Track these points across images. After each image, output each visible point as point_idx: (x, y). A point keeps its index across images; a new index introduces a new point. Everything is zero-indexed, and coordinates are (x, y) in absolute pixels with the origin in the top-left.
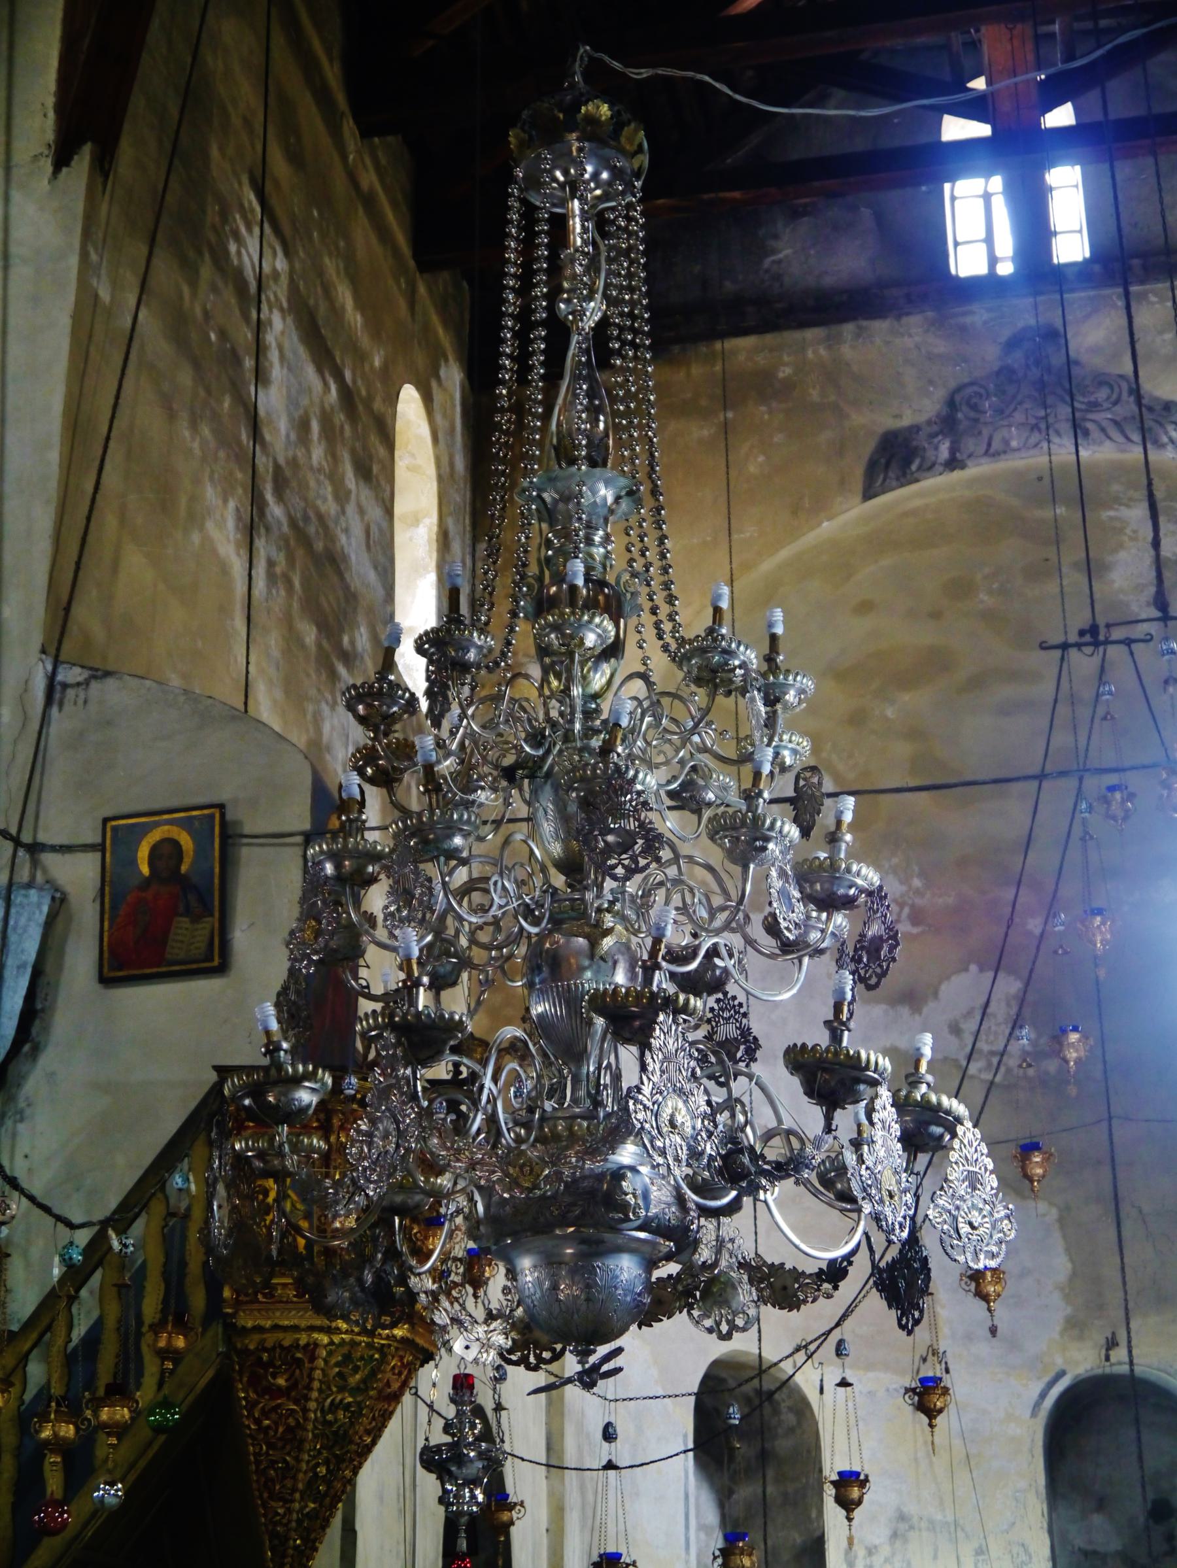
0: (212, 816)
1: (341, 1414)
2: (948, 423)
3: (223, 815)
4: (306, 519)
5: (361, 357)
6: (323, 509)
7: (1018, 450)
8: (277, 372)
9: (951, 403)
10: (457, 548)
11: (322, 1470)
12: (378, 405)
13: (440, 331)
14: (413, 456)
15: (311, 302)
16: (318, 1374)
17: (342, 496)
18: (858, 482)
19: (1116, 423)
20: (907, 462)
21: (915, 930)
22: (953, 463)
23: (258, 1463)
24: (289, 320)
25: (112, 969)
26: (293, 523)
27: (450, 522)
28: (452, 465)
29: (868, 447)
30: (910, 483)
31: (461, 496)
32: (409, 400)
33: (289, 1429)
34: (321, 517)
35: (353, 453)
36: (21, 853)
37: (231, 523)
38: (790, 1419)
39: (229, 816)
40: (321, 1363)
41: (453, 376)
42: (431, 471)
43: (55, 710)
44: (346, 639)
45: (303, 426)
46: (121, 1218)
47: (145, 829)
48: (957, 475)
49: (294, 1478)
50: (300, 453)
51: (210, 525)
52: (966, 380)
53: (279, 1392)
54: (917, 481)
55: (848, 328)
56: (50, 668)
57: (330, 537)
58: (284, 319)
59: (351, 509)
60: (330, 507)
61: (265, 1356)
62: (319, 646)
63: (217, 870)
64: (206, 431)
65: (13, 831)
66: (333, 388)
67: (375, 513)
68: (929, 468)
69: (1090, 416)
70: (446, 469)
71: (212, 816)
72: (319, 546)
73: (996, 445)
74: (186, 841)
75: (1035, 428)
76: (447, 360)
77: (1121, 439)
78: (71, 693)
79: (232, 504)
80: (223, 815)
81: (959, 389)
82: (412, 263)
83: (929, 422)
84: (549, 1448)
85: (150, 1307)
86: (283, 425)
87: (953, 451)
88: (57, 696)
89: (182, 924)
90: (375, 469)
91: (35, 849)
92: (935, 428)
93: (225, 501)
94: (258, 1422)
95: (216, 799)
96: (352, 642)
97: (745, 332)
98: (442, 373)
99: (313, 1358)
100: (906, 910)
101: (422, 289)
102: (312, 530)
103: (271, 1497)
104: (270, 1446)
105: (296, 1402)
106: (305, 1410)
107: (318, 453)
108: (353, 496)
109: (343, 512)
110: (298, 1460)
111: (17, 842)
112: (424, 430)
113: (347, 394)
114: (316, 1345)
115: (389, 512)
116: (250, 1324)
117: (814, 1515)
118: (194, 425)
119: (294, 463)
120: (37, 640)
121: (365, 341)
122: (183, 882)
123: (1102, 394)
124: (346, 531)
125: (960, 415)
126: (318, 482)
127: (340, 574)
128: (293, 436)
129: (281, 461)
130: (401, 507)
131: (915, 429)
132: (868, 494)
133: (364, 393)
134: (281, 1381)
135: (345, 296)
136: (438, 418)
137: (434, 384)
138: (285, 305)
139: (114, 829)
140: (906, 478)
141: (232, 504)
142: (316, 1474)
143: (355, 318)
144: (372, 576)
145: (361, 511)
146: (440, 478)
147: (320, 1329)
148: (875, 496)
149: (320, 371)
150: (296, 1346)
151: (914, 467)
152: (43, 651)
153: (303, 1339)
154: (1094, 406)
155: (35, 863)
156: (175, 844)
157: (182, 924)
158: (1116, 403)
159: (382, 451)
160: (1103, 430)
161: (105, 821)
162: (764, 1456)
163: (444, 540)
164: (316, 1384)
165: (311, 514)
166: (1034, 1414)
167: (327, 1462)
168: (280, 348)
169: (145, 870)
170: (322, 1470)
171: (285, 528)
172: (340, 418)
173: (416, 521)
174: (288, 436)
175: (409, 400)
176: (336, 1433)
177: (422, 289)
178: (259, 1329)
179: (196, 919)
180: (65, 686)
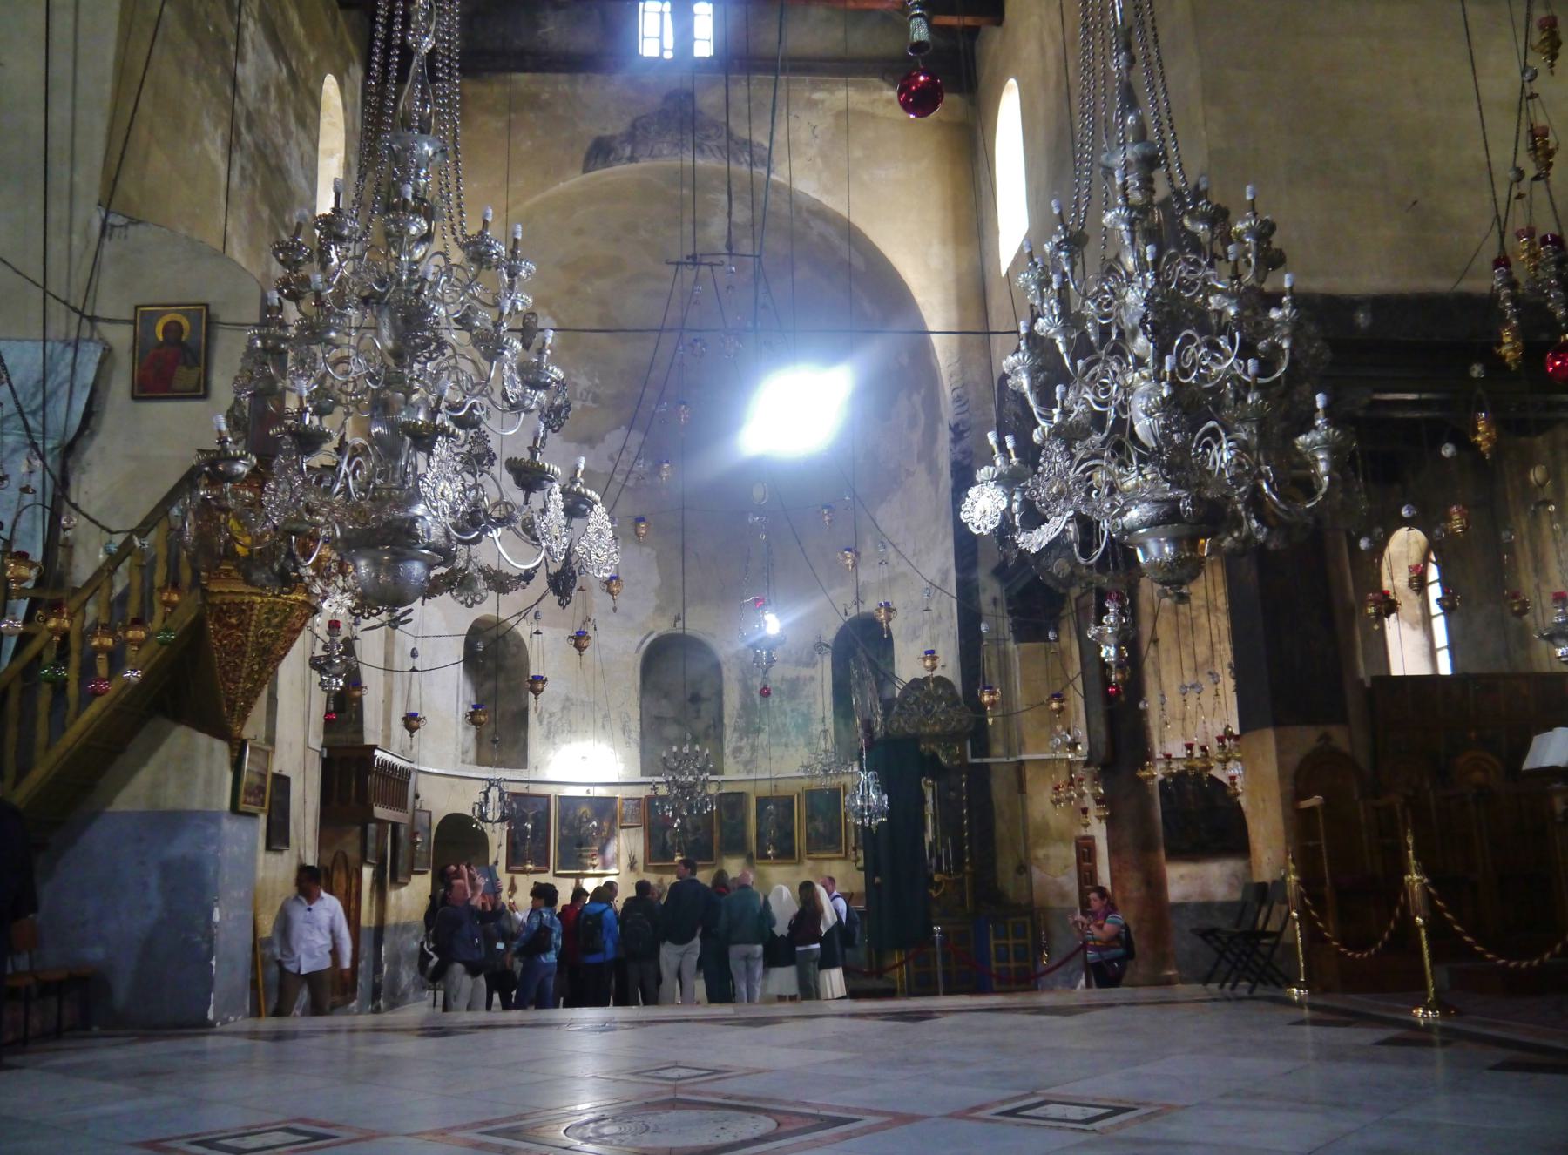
0: (201, 310)
1: (267, 639)
2: (631, 137)
3: (207, 310)
4: (265, 145)
5: (302, 54)
7: (667, 156)
8: (250, 56)
9: (634, 126)
11: (256, 667)
12: (311, 84)
14: (331, 116)
16: (254, 618)
17: (287, 134)
19: (718, 147)
21: (595, 406)
22: (632, 159)
23: (220, 663)
24: (259, 26)
26: (257, 146)
28: (354, 125)
29: (588, 143)
32: (330, 84)
33: (237, 646)
35: (295, 110)
36: (84, 321)
37: (219, 142)
38: (514, 650)
39: (212, 310)
40: (256, 612)
41: (357, 72)
42: (342, 126)
43: (106, 240)
44: (287, 218)
45: (265, 90)
46: (143, 530)
48: (633, 165)
49: (240, 671)
50: (263, 106)
51: (206, 142)
53: (232, 626)
54: (611, 166)
55: (581, 77)
56: (103, 214)
57: (278, 156)
58: (255, 24)
59: (292, 143)
60: (280, 140)
61: (225, 607)
62: (271, 221)
63: (203, 341)
64: (204, 84)
65: (80, 307)
66: (284, 70)
67: (307, 147)
68: (619, 160)
69: (707, 143)
70: (351, 127)
71: (201, 310)
72: (273, 162)
73: (656, 151)
74: (185, 323)
75: (676, 145)
76: (354, 63)
78: (117, 231)
83: (621, 135)
84: (386, 661)
85: (159, 578)
86: (253, 88)
88: (108, 231)
89: (182, 371)
90: (308, 121)
91: (93, 319)
93: (216, 128)
94: (220, 641)
95: (202, 301)
96: (291, 220)
97: (525, 70)
98: (351, 70)
99: (252, 610)
100: (590, 395)
102: (268, 151)
103: (227, 680)
104: (227, 654)
105: (242, 632)
106: (247, 636)
107: (274, 108)
108: (294, 135)
109: (288, 143)
110: (242, 662)
111: (82, 315)
112: (338, 102)
113: (293, 76)
114: (254, 602)
116: (216, 590)
117: (524, 697)
118: (197, 81)
119: (259, 111)
120: (96, 197)
121: (305, 44)
122: (183, 346)
123: (712, 132)
124: (290, 155)
125: (638, 133)
127: (285, 180)
128: (259, 95)
129: (251, 108)
130: (323, 145)
131: (613, 138)
132: (586, 170)
133: (303, 75)
134: (234, 621)
136: (348, 97)
137: (345, 76)
138: (256, 15)
139: (142, 312)
141: (220, 131)
142: (253, 670)
143: (299, 30)
144: (304, 183)
145: (299, 145)
146: (347, 131)
147: (257, 594)
149: (276, 57)
151: (611, 158)
152: (100, 204)
153: (247, 599)
154: (708, 137)
155: (93, 328)
156: (179, 325)
157: (182, 371)
159: (312, 111)
160: (711, 150)
161: (137, 307)
162: (499, 668)
164: (253, 623)
165: (268, 143)
166: (637, 651)
167: (259, 664)
168: (253, 42)
169: (160, 337)
170: (256, 667)
171: (252, 149)
172: (288, 88)
173: (331, 154)
174: (256, 94)
175: (330, 84)
176: (264, 649)
178: (221, 593)
180: (113, 226)
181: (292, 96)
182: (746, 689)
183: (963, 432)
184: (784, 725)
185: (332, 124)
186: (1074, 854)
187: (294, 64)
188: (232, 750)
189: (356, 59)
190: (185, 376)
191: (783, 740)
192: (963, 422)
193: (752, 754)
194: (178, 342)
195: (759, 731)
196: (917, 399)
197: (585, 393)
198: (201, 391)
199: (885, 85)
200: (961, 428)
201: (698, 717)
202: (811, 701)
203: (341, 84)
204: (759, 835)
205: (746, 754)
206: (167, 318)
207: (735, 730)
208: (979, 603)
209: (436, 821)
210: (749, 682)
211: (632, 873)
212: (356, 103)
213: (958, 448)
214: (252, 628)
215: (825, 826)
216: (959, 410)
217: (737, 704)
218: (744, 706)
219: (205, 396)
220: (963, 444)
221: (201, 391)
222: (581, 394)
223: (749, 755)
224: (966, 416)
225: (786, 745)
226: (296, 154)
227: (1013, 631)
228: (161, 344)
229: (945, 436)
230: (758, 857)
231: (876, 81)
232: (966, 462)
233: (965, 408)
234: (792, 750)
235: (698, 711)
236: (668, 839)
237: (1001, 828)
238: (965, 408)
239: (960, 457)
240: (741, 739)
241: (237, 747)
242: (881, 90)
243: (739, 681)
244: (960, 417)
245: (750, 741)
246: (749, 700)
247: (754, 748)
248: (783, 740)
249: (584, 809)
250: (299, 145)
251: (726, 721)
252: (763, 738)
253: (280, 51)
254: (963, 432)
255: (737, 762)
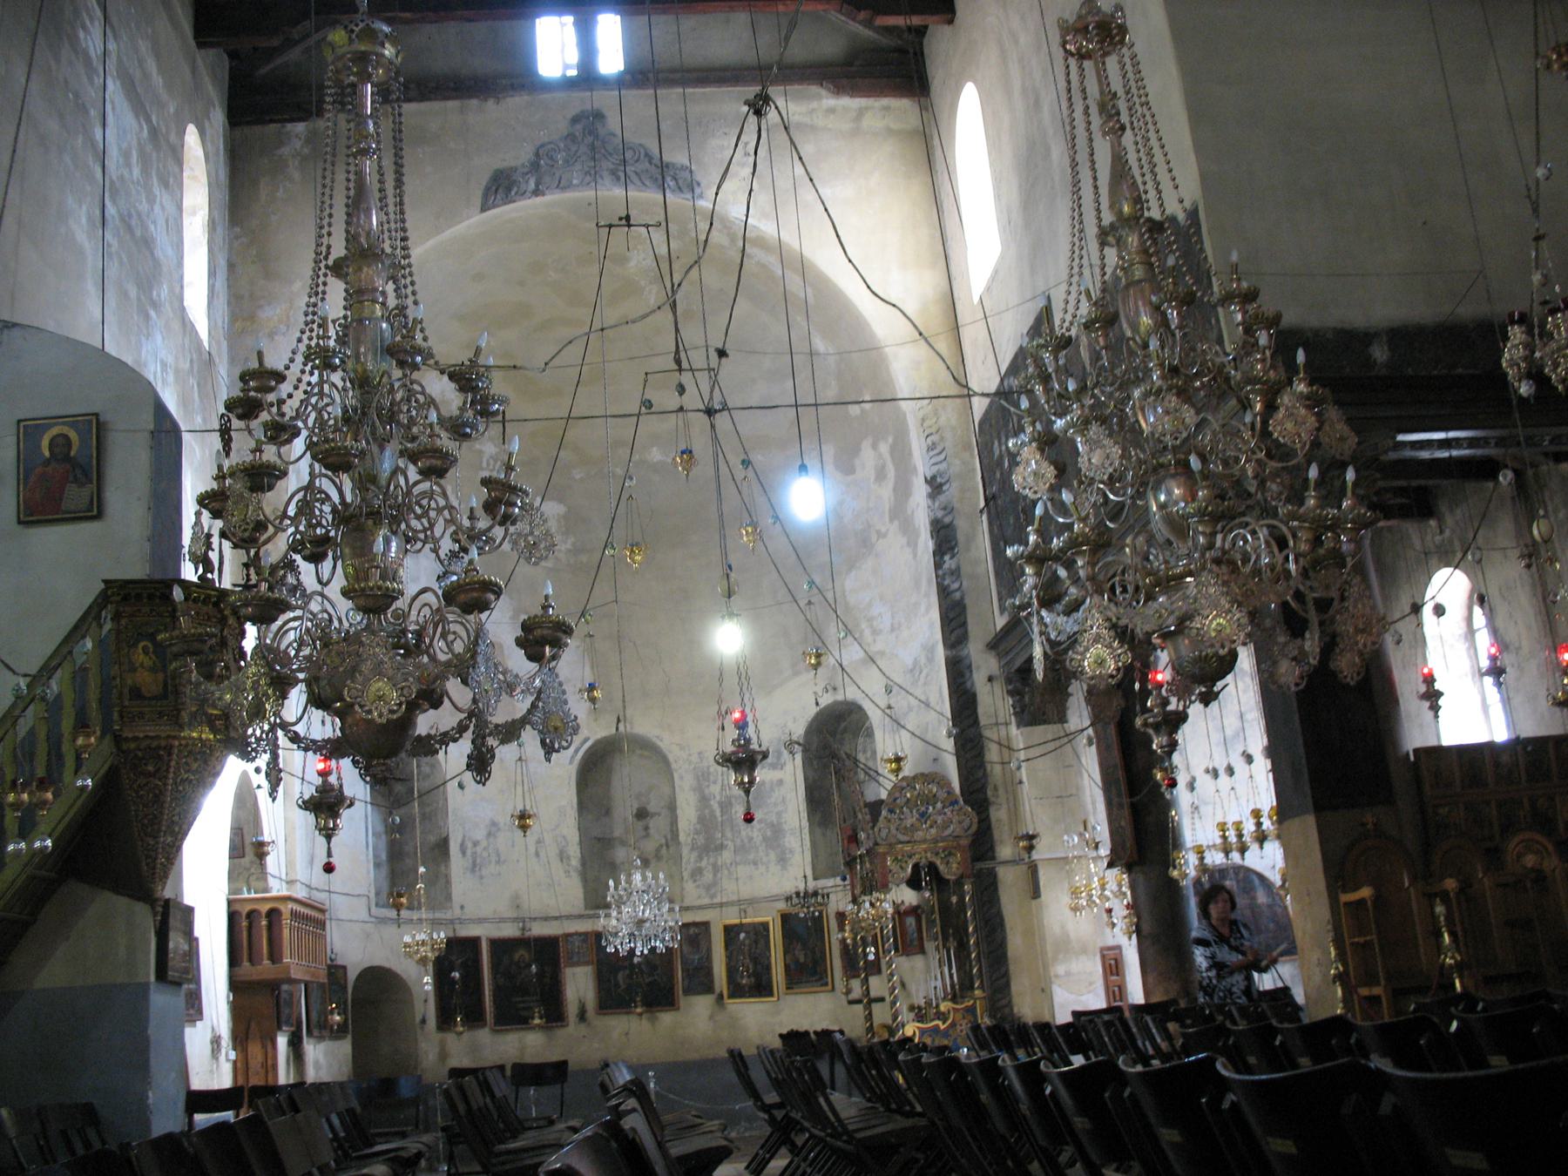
0: (90, 422)
2: (535, 166)
3: (98, 420)
4: (130, 216)
6: (140, 208)
9: (537, 155)
10: (219, 230)
12: (173, 138)
13: (210, 88)
14: (192, 169)
15: (131, 71)
17: (151, 200)
18: (478, 201)
19: (636, 173)
20: (509, 189)
22: (537, 192)
24: (118, 83)
25: (25, 515)
26: (122, 219)
27: (216, 213)
29: (485, 179)
30: (510, 202)
31: (223, 196)
32: (192, 136)
34: (139, 215)
37: (84, 221)
39: (101, 419)
41: (218, 117)
42: (204, 180)
44: (155, 293)
45: (126, 155)
46: (48, 670)
47: (49, 427)
48: (538, 200)
49: (160, 823)
52: (546, 140)
53: (150, 775)
55: (474, 102)
57: (145, 227)
59: (157, 208)
61: (140, 754)
62: (139, 299)
67: (171, 208)
71: (90, 422)
72: (138, 233)
73: (563, 183)
74: (73, 435)
77: (639, 183)
79: (84, 207)
80: (98, 420)
81: (542, 146)
82: (192, 43)
83: (523, 165)
85: (67, 724)
87: (537, 184)
90: (171, 180)
92: (526, 170)
93: (80, 207)
94: (137, 792)
95: (89, 411)
96: (159, 296)
99: (170, 754)
101: (199, 61)
105: (160, 780)
106: (165, 784)
107: (136, 172)
112: (200, 153)
113: (154, 132)
115: (180, 208)
116: (130, 735)
119: (122, 178)
121: (164, 96)
124: (154, 222)
126: (138, 192)
128: (121, 160)
130: (187, 202)
132: (484, 209)
133: (164, 131)
134: (150, 768)
135: (151, 65)
137: (207, 125)
140: (508, 200)
141: (84, 208)
143: (157, 80)
144: (170, 252)
145: (163, 207)
148: (489, 209)
149: (137, 116)
150: (159, 747)
153: (163, 743)
156: (66, 437)
158: (637, 161)
159: (177, 170)
163: (212, 225)
164: (172, 770)
166: (571, 763)
169: (47, 454)
172: (149, 148)
173: (194, 213)
175: (192, 136)
177: (199, 61)
178: (136, 739)
179: (82, 485)
181: (154, 155)
182: (704, 800)
183: (941, 485)
184: (751, 839)
185: (194, 178)
186: (1099, 969)
187: (154, 119)
188: (155, 915)
189: (217, 103)
190: (75, 496)
191: (751, 857)
192: (941, 474)
193: (715, 875)
194: (67, 458)
195: (722, 847)
196: (884, 448)
197: (492, 462)
198: (94, 511)
199: (824, 92)
200: (939, 480)
201: (647, 836)
202: (780, 808)
203: (202, 133)
204: (731, 972)
205: (708, 877)
206: (55, 431)
207: (693, 849)
208: (973, 684)
209: (352, 976)
210: (707, 791)
211: (583, 1026)
212: (218, 149)
213: (937, 504)
214: (171, 775)
215: (805, 955)
216: (933, 461)
217: (694, 820)
218: (701, 819)
219: (99, 516)
220: (942, 498)
221: (94, 511)
222: (488, 464)
223: (711, 876)
224: (943, 466)
225: (755, 863)
226: (161, 222)
227: (1015, 714)
228: (47, 462)
229: (920, 491)
230: (731, 996)
231: (814, 89)
232: (947, 520)
233: (942, 456)
234: (762, 869)
235: (646, 828)
236: (621, 982)
237: (1015, 943)
238: (942, 456)
239: (940, 514)
240: (700, 858)
241: (160, 909)
242: (820, 97)
243: (694, 790)
244: (935, 469)
245: (712, 860)
246: (707, 811)
247: (716, 869)
248: (751, 857)
249: (521, 954)
250: (163, 207)
251: (682, 837)
252: (727, 856)
253: (139, 109)
254: (941, 485)
255: (698, 887)
